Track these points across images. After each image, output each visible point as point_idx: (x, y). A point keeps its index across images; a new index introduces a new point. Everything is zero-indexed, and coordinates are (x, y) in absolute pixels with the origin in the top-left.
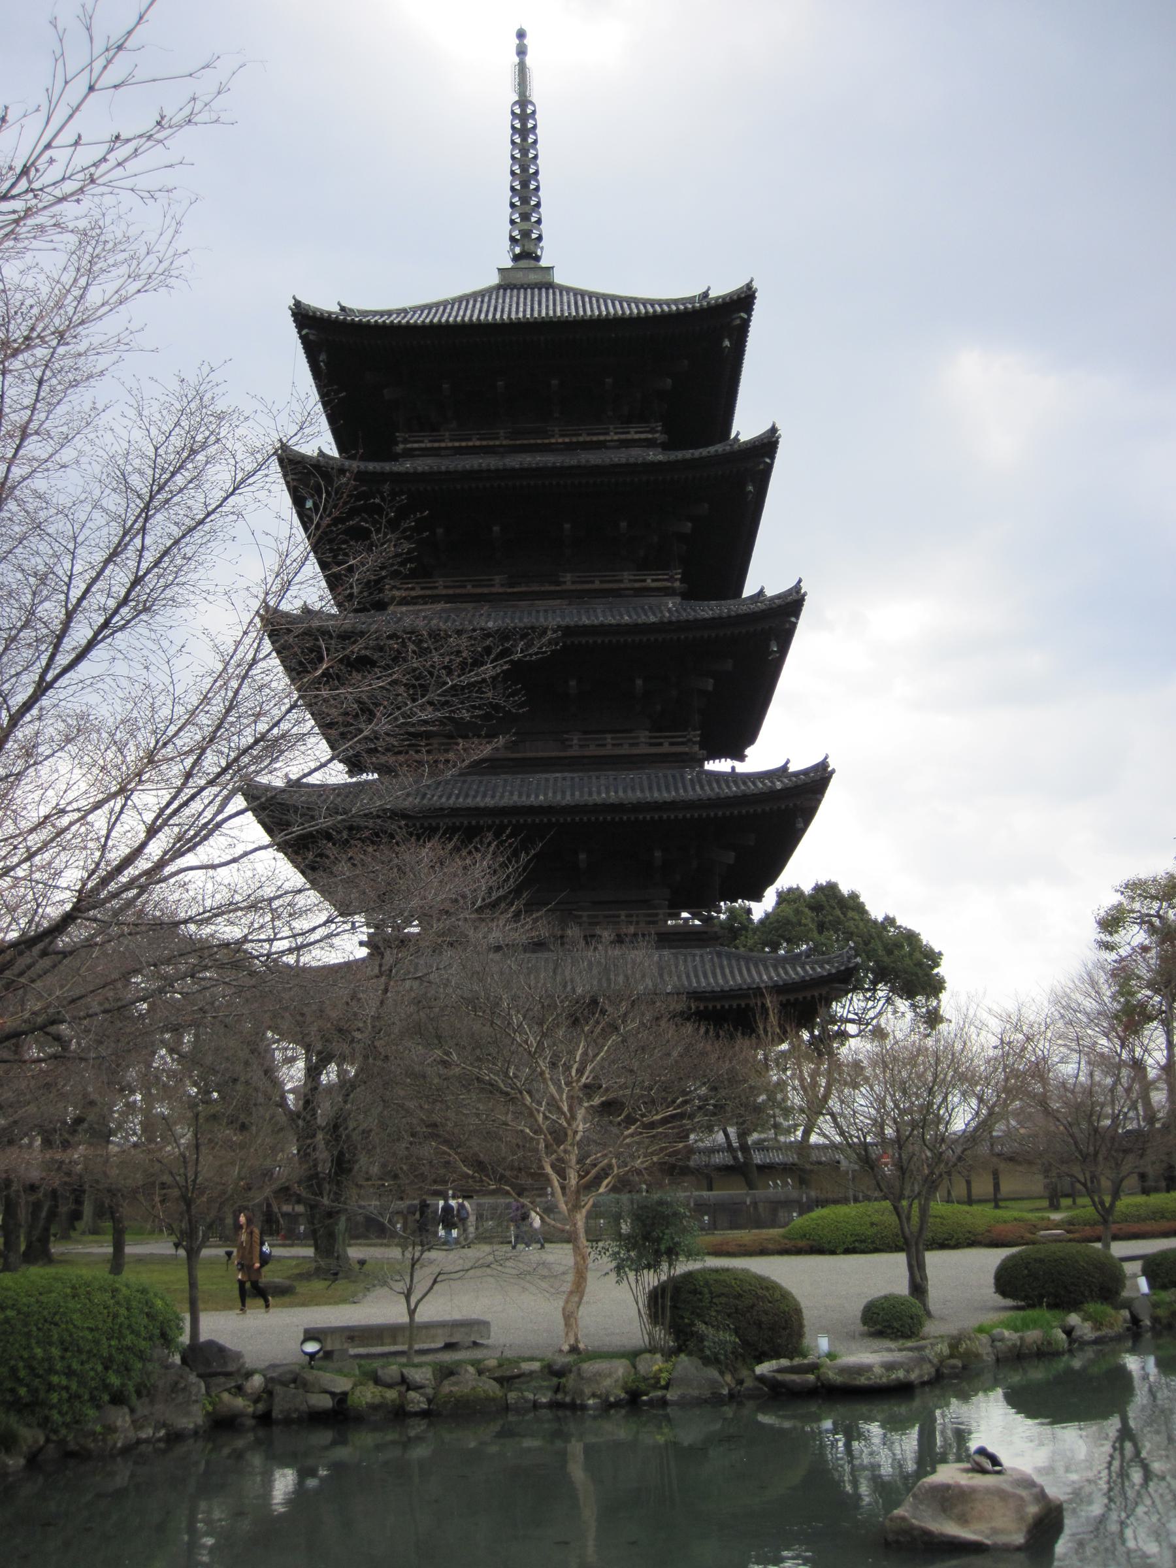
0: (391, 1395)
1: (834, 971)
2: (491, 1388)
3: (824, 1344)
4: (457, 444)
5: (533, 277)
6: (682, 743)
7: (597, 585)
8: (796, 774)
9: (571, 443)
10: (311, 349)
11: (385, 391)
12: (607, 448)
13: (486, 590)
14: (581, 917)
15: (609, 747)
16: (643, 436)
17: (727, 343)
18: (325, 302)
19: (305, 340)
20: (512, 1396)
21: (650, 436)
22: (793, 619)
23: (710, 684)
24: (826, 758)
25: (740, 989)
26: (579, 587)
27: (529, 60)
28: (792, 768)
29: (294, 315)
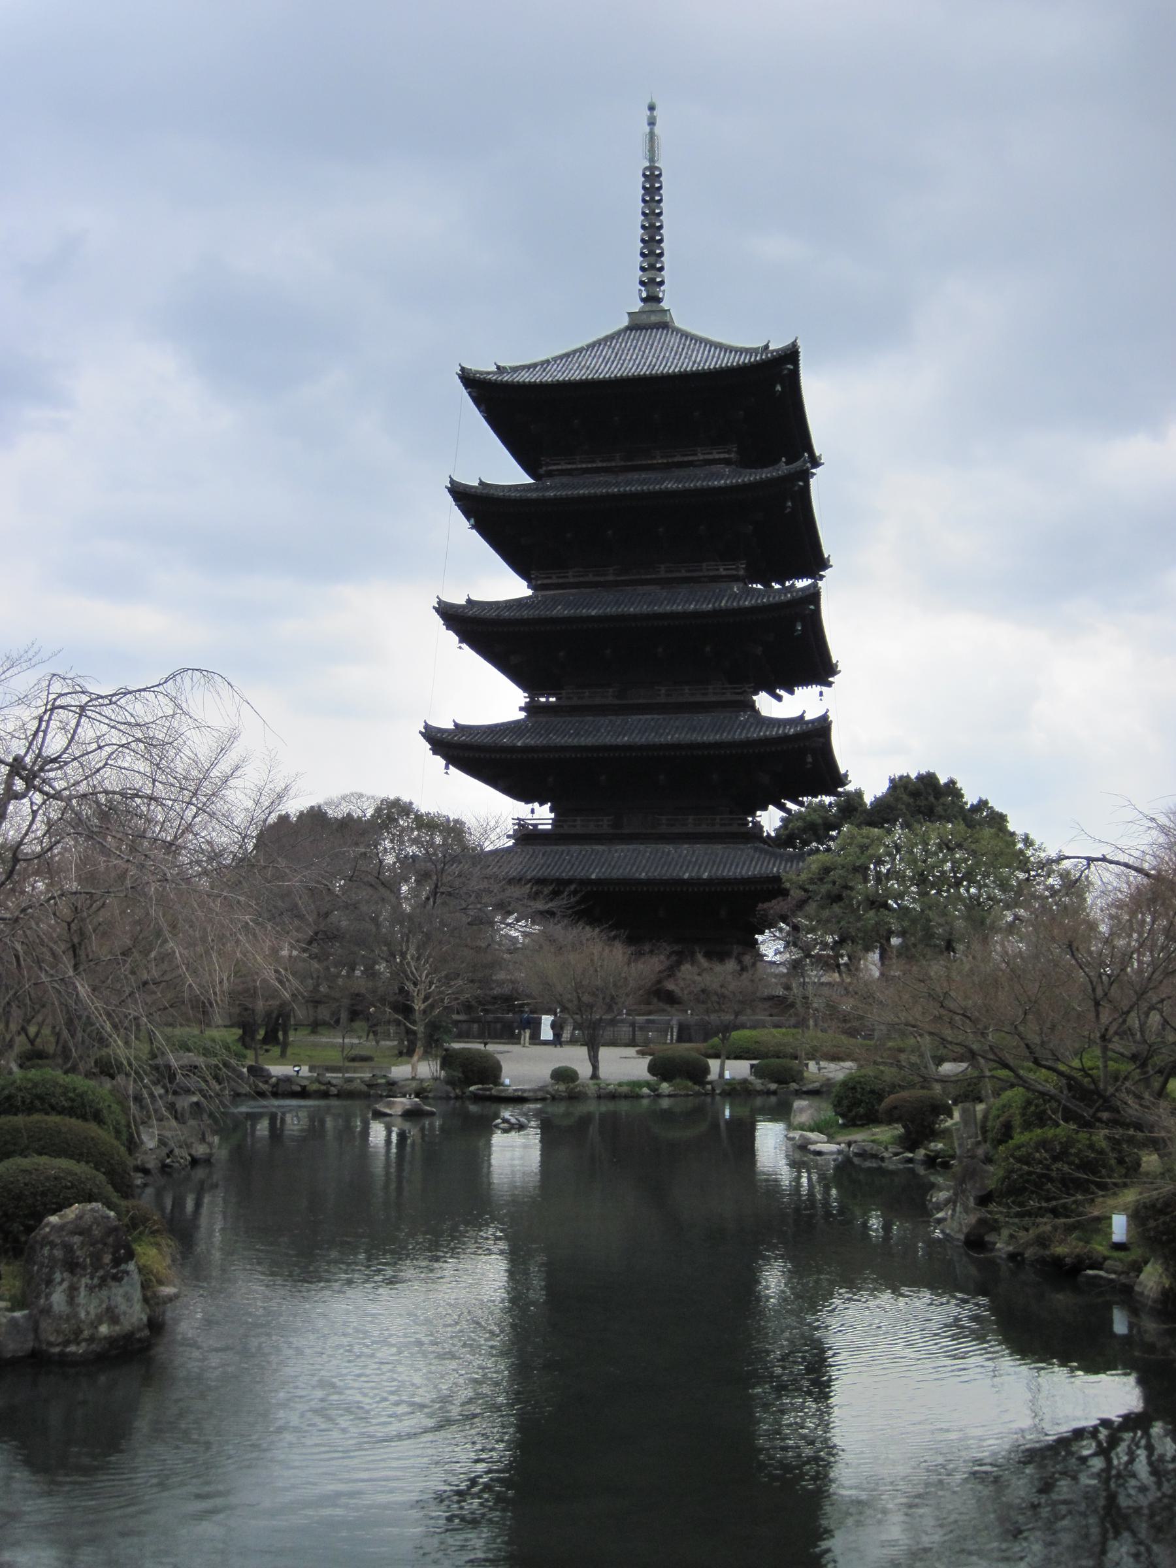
0: (323, 1087)
2: (364, 1088)
3: (507, 1081)
4: (584, 466)
5: (654, 319)
7: (684, 574)
8: (812, 721)
9: (668, 463)
10: (477, 401)
12: (695, 466)
13: (602, 579)
16: (722, 456)
17: (779, 388)
18: (484, 364)
20: (372, 1092)
21: (727, 456)
22: (812, 607)
26: (670, 575)
27: (657, 129)
28: (808, 717)
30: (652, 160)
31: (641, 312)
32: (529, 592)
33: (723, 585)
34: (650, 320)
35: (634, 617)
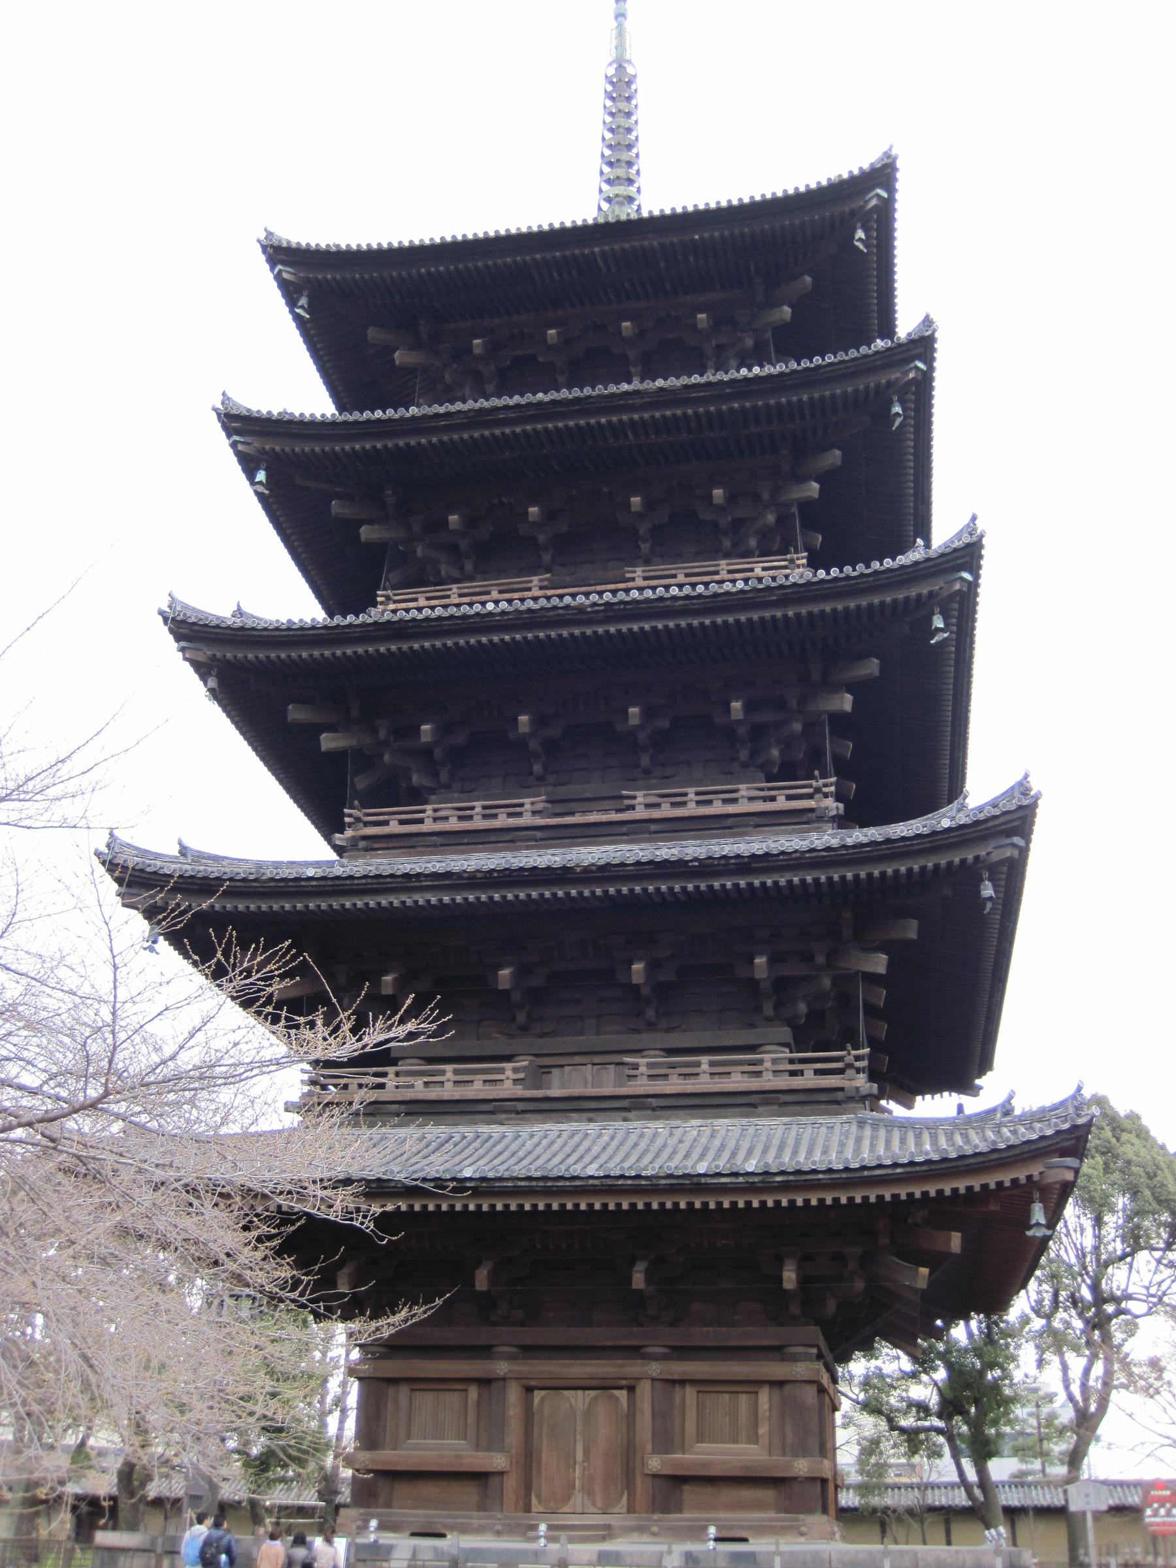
1: (1049, 1132)
6: (810, 796)
10: (290, 291)
11: (397, 354)
14: (635, 1067)
15: (692, 805)
19: (283, 285)
22: (966, 576)
23: (846, 702)
24: (1026, 776)
25: (880, 1166)
27: (628, 24)
29: (264, 248)
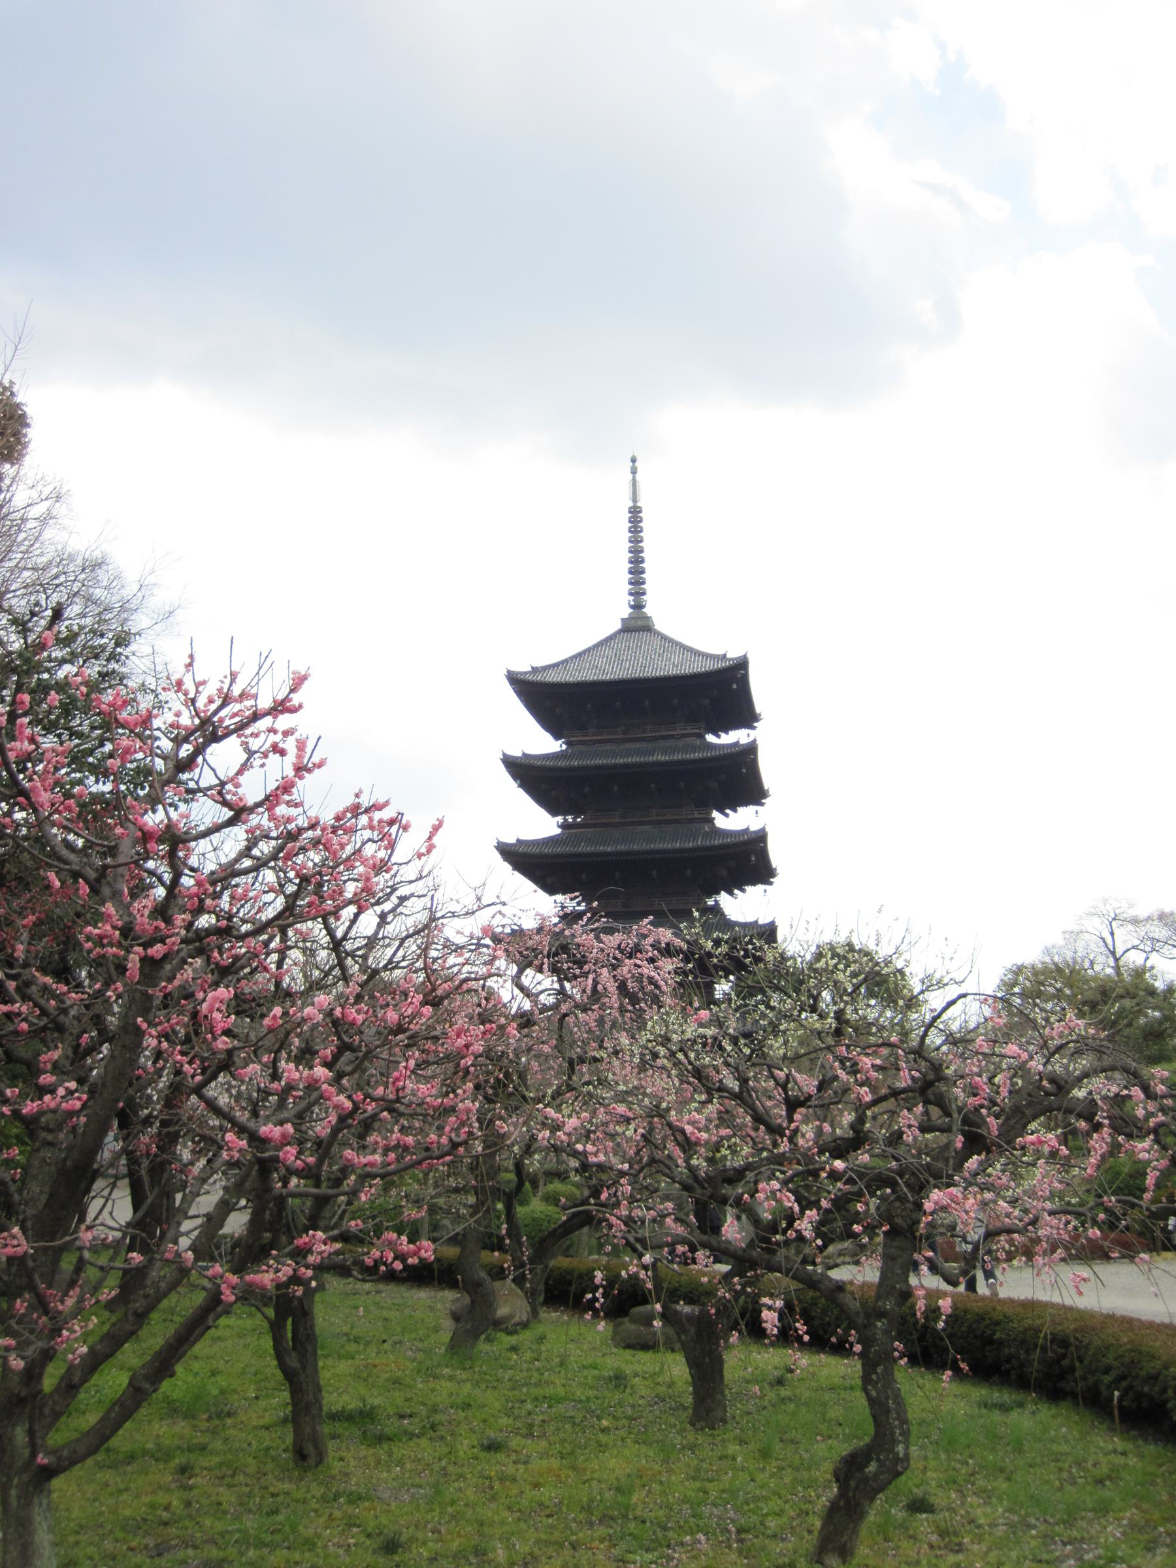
5: (640, 623)
7: (668, 817)
17: (735, 686)
18: (522, 666)
27: (637, 476)
28: (761, 922)
30: (635, 500)
31: (630, 618)
32: (559, 831)
33: (698, 826)
34: (637, 625)
35: (638, 853)
